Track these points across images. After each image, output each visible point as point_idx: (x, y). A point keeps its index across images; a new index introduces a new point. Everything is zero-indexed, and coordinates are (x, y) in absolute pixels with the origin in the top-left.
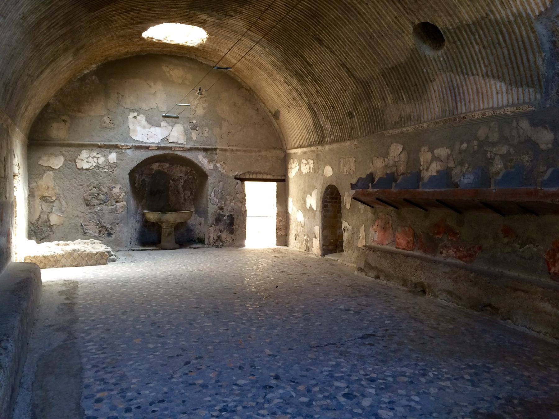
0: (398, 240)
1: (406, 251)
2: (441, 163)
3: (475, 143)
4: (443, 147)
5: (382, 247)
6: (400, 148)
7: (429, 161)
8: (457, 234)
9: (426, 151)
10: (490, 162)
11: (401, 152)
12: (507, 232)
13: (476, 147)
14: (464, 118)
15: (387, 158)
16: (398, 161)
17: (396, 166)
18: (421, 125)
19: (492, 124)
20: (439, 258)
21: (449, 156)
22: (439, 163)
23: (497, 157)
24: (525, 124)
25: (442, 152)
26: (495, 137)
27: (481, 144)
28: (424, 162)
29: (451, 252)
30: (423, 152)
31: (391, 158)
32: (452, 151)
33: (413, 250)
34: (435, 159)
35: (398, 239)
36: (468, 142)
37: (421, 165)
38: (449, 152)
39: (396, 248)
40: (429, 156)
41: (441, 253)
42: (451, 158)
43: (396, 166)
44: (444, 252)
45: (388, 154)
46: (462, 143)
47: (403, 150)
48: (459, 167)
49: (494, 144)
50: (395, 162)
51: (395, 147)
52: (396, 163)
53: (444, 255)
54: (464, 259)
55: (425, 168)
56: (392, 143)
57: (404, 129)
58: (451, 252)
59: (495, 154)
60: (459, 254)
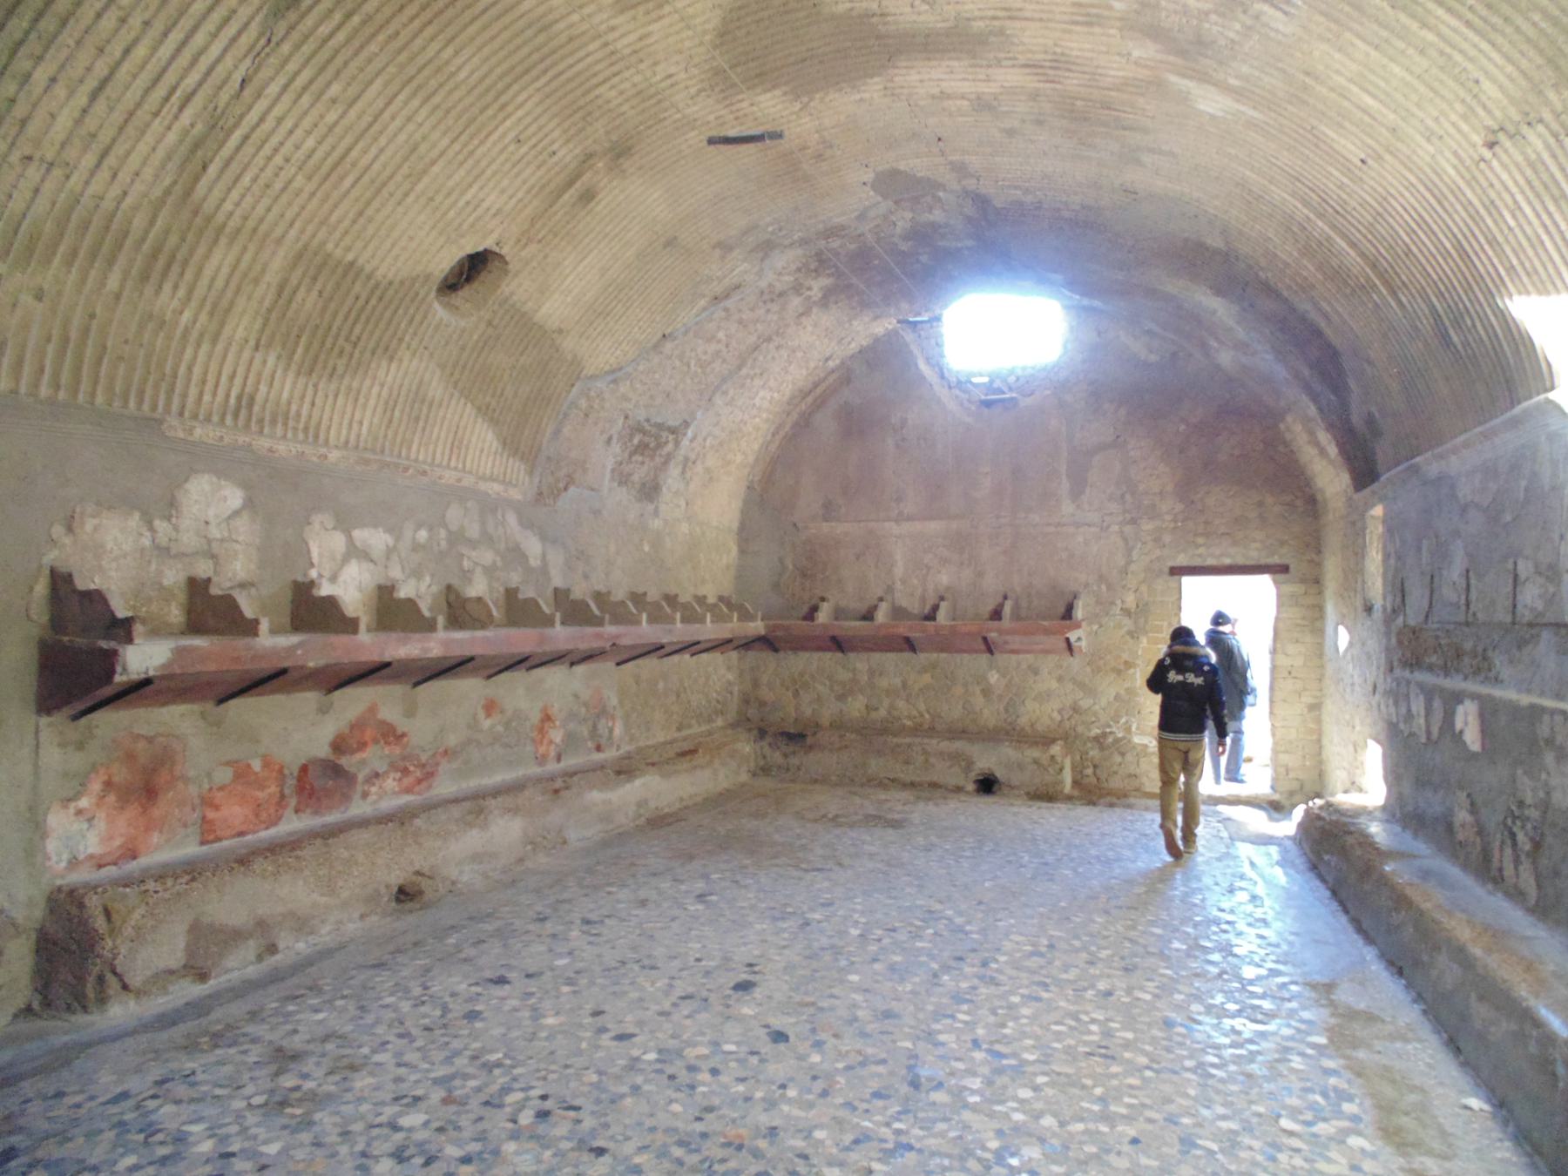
0: (211, 815)
1: (249, 838)
2: (371, 566)
3: (443, 533)
4: (375, 526)
5: (144, 861)
6: (234, 498)
7: (339, 557)
8: (403, 735)
9: (330, 526)
10: (467, 576)
11: (237, 513)
12: (490, 707)
13: (443, 544)
14: (424, 473)
15: (169, 518)
16: (222, 540)
17: (213, 557)
18: (323, 450)
19: (469, 504)
20: (358, 808)
21: (389, 552)
22: (366, 565)
23: (479, 570)
24: (512, 519)
25: (375, 539)
26: (473, 531)
27: (456, 538)
28: (321, 555)
29: (390, 783)
30: (317, 526)
31: (185, 523)
32: (398, 539)
33: (274, 822)
34: (355, 552)
35: (217, 808)
36: (431, 529)
37: (312, 565)
38: (391, 542)
39: (203, 843)
40: (338, 541)
41: (365, 795)
42: (395, 557)
43: (213, 557)
44: (374, 789)
45: (172, 503)
46: (419, 527)
47: (244, 507)
48: (412, 582)
49: (473, 544)
50: (209, 542)
51: (207, 487)
52: (214, 545)
53: (372, 798)
54: (417, 789)
55: (327, 574)
56: (193, 471)
57: (263, 443)
58: (390, 783)
59: (476, 564)
60: (407, 781)
